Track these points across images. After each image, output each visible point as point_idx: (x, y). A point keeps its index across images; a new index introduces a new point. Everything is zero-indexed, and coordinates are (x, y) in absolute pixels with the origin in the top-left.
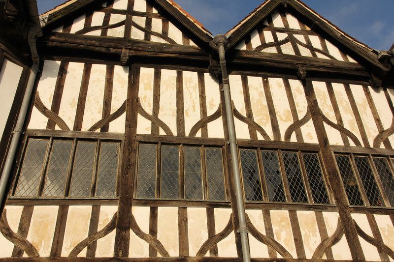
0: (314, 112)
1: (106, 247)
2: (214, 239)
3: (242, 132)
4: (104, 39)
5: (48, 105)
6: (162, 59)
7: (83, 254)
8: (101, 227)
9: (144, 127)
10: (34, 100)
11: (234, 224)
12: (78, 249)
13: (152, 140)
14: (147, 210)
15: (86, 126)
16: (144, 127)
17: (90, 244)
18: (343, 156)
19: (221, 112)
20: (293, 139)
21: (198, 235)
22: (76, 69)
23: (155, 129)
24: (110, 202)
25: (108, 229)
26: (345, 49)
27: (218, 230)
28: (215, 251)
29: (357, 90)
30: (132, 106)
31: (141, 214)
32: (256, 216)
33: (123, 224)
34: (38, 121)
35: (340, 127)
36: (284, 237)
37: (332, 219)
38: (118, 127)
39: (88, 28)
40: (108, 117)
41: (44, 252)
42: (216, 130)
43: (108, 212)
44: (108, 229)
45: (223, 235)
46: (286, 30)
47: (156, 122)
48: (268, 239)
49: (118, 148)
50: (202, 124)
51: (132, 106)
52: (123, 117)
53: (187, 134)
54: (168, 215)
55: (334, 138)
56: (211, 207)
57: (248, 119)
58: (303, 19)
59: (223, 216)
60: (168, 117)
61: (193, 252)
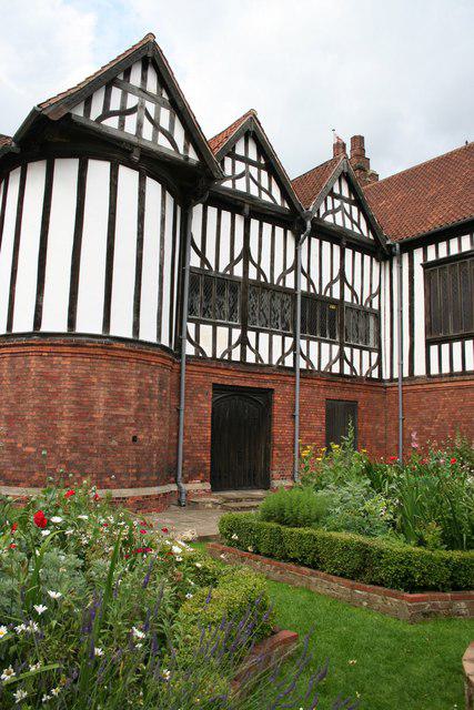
1: (236, 356)
2: (284, 355)
4: (234, 192)
8: (234, 342)
9: (253, 274)
11: (294, 347)
13: (257, 284)
14: (254, 333)
15: (221, 270)
17: (229, 351)
19: (295, 266)
20: (328, 295)
23: (259, 277)
24: (237, 327)
25: (237, 344)
26: (370, 227)
27: (286, 351)
28: (283, 362)
29: (367, 258)
31: (251, 335)
32: (303, 343)
33: (243, 341)
34: (194, 261)
35: (352, 288)
36: (314, 358)
40: (233, 262)
41: (209, 355)
43: (237, 333)
44: (237, 344)
45: (288, 354)
46: (339, 197)
47: (260, 272)
50: (283, 277)
52: (241, 261)
54: (264, 337)
55: (348, 298)
56: (284, 336)
58: (352, 189)
59: (289, 341)
61: (274, 363)
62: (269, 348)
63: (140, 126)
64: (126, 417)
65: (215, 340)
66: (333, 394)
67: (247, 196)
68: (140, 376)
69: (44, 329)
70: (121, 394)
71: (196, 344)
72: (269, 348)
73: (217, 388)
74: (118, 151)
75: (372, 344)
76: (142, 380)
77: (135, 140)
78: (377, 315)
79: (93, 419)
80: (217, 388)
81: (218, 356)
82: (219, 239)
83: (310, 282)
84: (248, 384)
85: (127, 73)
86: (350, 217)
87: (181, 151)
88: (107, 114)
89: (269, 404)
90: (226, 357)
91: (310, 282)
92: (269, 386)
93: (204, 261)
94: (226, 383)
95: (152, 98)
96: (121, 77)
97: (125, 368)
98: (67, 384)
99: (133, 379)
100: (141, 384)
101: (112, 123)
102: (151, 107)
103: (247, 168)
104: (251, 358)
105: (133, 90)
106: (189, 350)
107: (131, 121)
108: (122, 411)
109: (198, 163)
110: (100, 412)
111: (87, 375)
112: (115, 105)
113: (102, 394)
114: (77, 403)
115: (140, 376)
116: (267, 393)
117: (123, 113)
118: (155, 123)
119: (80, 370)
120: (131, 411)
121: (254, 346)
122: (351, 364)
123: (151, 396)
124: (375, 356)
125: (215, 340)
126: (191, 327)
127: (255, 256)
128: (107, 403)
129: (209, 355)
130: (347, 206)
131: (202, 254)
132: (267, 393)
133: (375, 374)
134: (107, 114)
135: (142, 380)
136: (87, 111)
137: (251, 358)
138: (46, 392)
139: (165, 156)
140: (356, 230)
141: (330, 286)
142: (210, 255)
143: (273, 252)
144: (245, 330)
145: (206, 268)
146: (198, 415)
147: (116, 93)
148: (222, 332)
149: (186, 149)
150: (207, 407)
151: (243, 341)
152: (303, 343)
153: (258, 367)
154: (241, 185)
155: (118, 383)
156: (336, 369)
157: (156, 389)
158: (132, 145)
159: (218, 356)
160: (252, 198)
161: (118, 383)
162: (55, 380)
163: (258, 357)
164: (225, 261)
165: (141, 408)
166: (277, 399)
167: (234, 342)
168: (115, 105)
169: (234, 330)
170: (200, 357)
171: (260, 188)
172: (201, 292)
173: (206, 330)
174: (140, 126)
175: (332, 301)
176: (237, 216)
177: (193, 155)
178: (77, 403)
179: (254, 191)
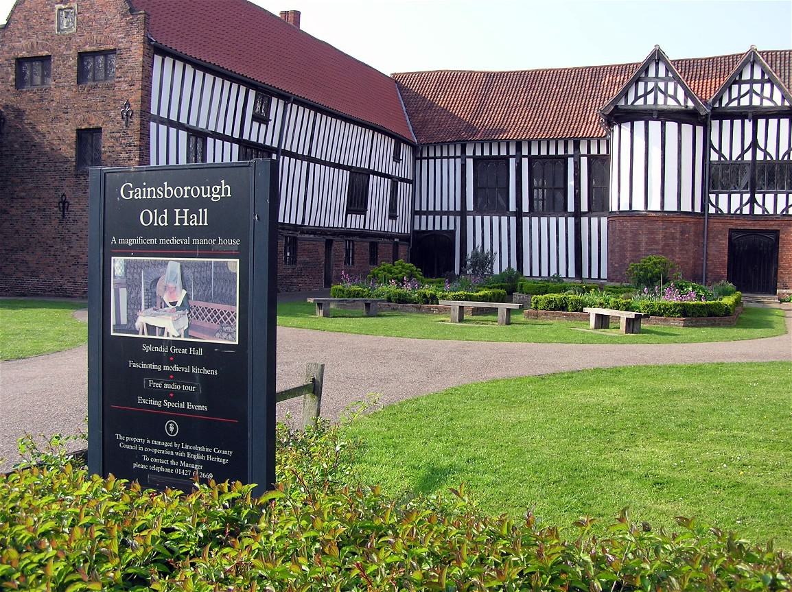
1: (746, 210)
4: (739, 107)
5: (717, 149)
7: (738, 212)
8: (744, 203)
10: (712, 146)
12: (737, 210)
15: (734, 159)
16: (760, 156)
22: (726, 123)
23: (765, 157)
25: (746, 204)
30: (755, 144)
31: (759, 197)
33: (752, 201)
34: (714, 157)
38: (748, 156)
39: (731, 100)
40: (744, 152)
41: (725, 211)
43: (746, 197)
44: (746, 204)
47: (766, 153)
49: (748, 169)
51: (755, 144)
53: (780, 159)
54: (770, 198)
60: (771, 149)
61: (779, 212)
62: (775, 203)
63: (656, 99)
64: (656, 250)
65: (729, 203)
67: (751, 107)
68: (665, 229)
69: (621, 209)
70: (654, 239)
71: (716, 206)
72: (775, 203)
74: (646, 115)
76: (667, 231)
77: (654, 107)
79: (640, 251)
81: (732, 212)
82: (731, 141)
84: (757, 228)
85: (647, 71)
87: (682, 104)
88: (637, 98)
89: (777, 239)
90: (738, 212)
92: (775, 228)
93: (721, 155)
94: (739, 228)
95: (662, 79)
96: (643, 75)
98: (629, 235)
100: (666, 233)
101: (640, 102)
102: (661, 85)
103: (751, 87)
104: (758, 211)
105: (651, 79)
106: (712, 210)
107: (650, 98)
108: (654, 247)
109: (694, 107)
111: (637, 230)
112: (641, 92)
114: (633, 244)
115: (665, 229)
116: (777, 232)
117: (646, 94)
118: (665, 93)
119: (635, 228)
120: (660, 247)
121: (761, 204)
123: (673, 239)
125: (729, 203)
126: (712, 197)
127: (761, 143)
128: (646, 243)
129: (725, 211)
131: (719, 152)
134: (637, 98)
135: (667, 231)
136: (626, 102)
137: (758, 211)
138: (621, 238)
139: (672, 110)
145: (722, 159)
146: (719, 250)
147: (641, 85)
148: (735, 198)
149: (686, 101)
150: (725, 243)
151: (752, 201)
153: (765, 216)
154: (745, 102)
155: (652, 233)
157: (678, 235)
158: (652, 110)
159: (732, 212)
160: (755, 107)
161: (652, 233)
162: (624, 233)
163: (765, 210)
167: (744, 203)
168: (641, 92)
169: (744, 195)
173: (723, 198)
174: (656, 99)
176: (746, 121)
177: (690, 104)
178: (633, 244)
179: (756, 101)
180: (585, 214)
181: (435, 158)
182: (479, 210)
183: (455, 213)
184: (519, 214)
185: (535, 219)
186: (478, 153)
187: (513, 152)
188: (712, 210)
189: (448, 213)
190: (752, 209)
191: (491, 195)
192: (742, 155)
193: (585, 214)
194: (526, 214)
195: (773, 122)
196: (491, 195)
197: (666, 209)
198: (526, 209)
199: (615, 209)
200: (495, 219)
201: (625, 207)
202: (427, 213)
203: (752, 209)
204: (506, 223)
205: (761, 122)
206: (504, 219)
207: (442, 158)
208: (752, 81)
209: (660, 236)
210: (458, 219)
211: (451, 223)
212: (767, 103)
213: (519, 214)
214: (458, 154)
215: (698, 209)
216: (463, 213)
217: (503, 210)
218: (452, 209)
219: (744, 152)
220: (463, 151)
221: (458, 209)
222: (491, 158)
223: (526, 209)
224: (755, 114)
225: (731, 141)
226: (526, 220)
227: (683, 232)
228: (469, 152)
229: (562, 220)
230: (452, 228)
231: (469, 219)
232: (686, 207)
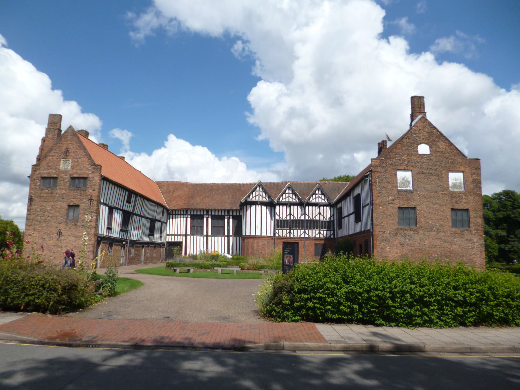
0: (320, 214)
1: (288, 235)
3: (307, 218)
6: (294, 204)
13: (293, 221)
16: (292, 218)
18: (322, 221)
21: (299, 234)
30: (290, 214)
31: (292, 231)
33: (290, 232)
34: (277, 217)
36: (310, 234)
37: (318, 232)
40: (287, 216)
42: (303, 218)
43: (288, 231)
47: (294, 217)
48: (308, 235)
51: (290, 214)
54: (295, 231)
55: (322, 218)
57: (308, 215)
60: (296, 216)
62: (297, 233)
65: (283, 233)
66: (317, 242)
67: (289, 202)
72: (297, 233)
73: (283, 242)
75: (332, 229)
78: (333, 221)
80: (283, 242)
82: (282, 212)
83: (309, 217)
86: (321, 198)
91: (309, 217)
97: (259, 240)
99: (261, 242)
106: (277, 235)
110: (255, 248)
113: (255, 245)
116: (298, 243)
122: (308, 235)
124: (332, 232)
125: (283, 233)
126: (277, 231)
127: (292, 214)
130: (320, 196)
132: (298, 243)
133: (332, 237)
137: (292, 236)
140: (323, 201)
141: (316, 217)
142: (281, 216)
143: (297, 213)
144: (290, 230)
148: (285, 231)
151: (290, 232)
152: (307, 231)
153: (294, 238)
156: (318, 236)
157: (266, 244)
164: (285, 216)
165: (263, 247)
166: (299, 244)
170: (280, 238)
171: (292, 199)
172: (280, 224)
173: (281, 231)
175: (317, 221)
179: (291, 200)
180: (231, 236)
181: (175, 215)
182: (192, 234)
183: (183, 235)
184: (207, 236)
185: (213, 238)
186: (192, 213)
187: (205, 213)
188: (277, 235)
189: (180, 235)
190: (290, 235)
191: (197, 230)
192: (286, 217)
193: (231, 236)
194: (210, 236)
195: (296, 207)
196: (197, 230)
197: (263, 235)
198: (210, 234)
199: (244, 234)
200: (198, 237)
201: (248, 234)
202: (172, 235)
203: (290, 235)
204: (203, 239)
205: (292, 207)
206: (202, 237)
207: (178, 214)
208: (289, 193)
209: (260, 244)
210: (184, 237)
211: (182, 239)
212: (294, 201)
213: (207, 236)
214: (185, 213)
215: (272, 235)
216: (186, 235)
217: (202, 234)
218: (182, 233)
219: (287, 216)
220: (187, 212)
221: (184, 233)
222: (197, 215)
223: (210, 234)
224: (289, 204)
225: (282, 212)
226: (209, 238)
227: (268, 243)
228: (189, 213)
229: (223, 238)
230: (181, 240)
231: (188, 237)
232: (269, 235)
